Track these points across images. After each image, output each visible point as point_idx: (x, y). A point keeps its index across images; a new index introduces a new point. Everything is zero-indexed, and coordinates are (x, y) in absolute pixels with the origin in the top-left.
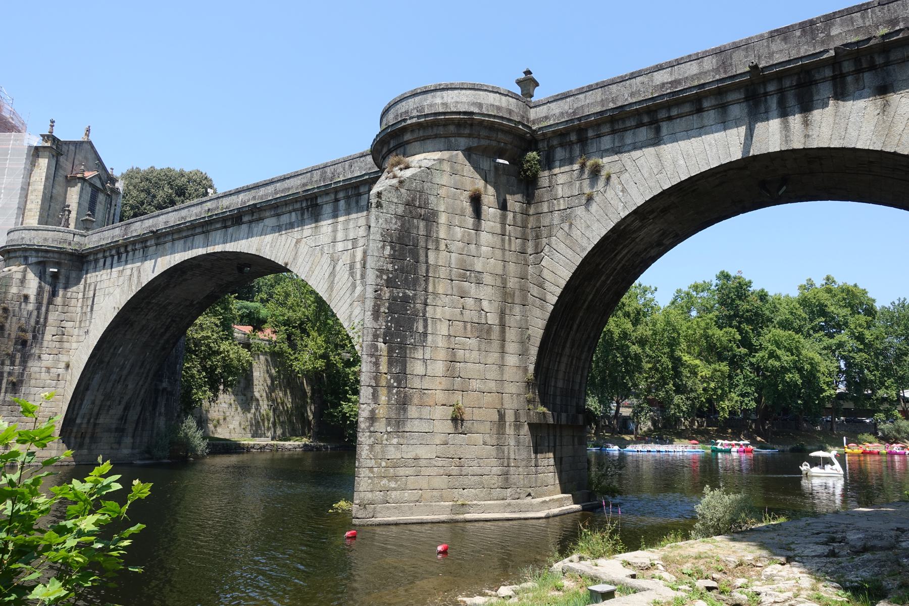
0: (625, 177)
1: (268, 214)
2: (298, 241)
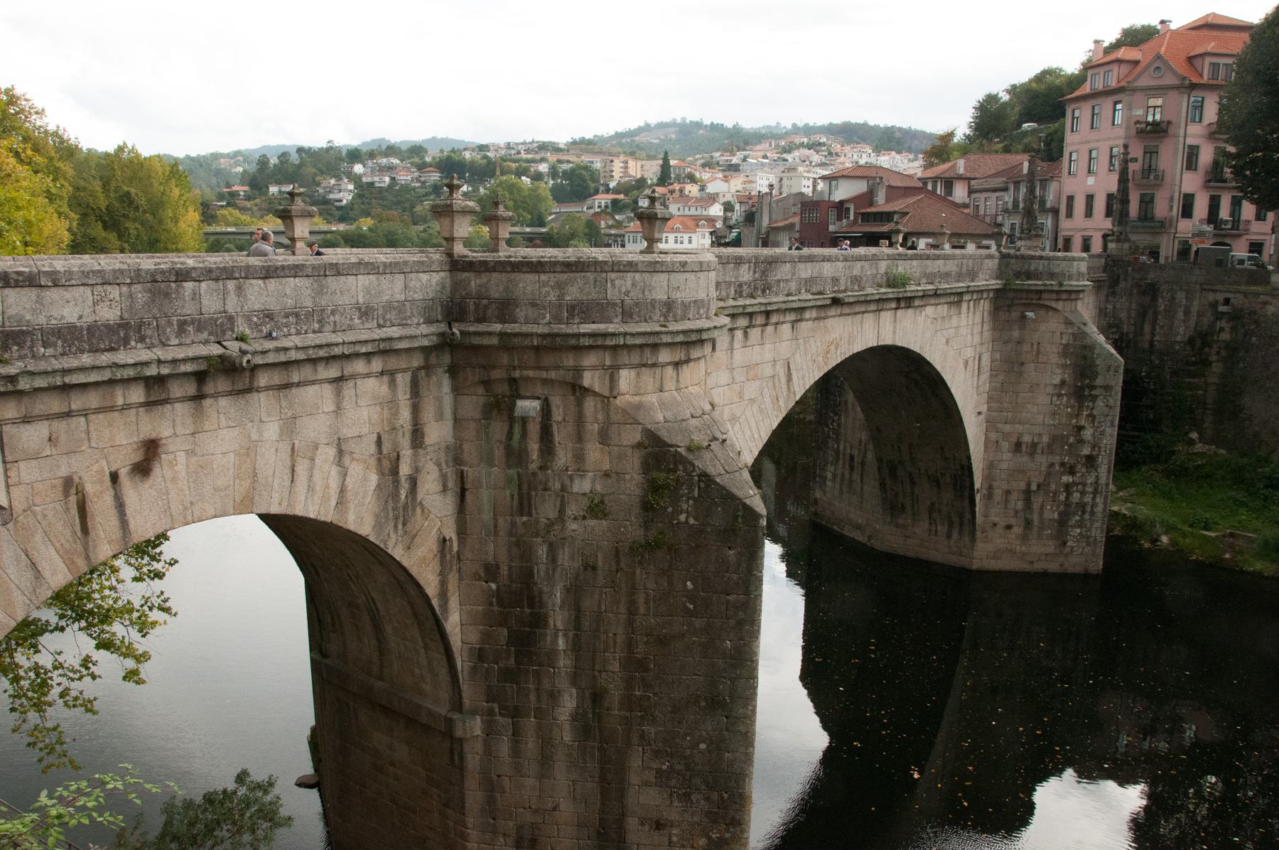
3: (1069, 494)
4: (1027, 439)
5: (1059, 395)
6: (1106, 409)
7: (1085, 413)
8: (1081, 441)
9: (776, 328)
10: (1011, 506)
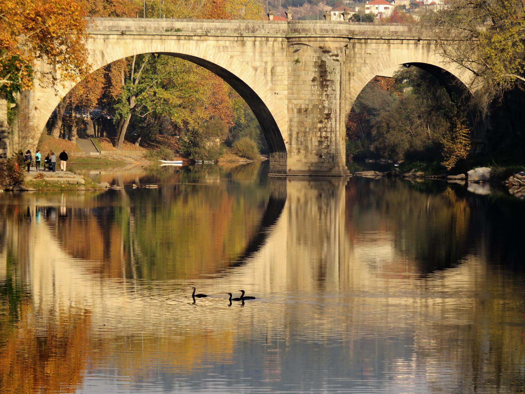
0: (379, 60)
4: (303, 107)
6: (332, 91)
7: (325, 93)
10: (299, 139)
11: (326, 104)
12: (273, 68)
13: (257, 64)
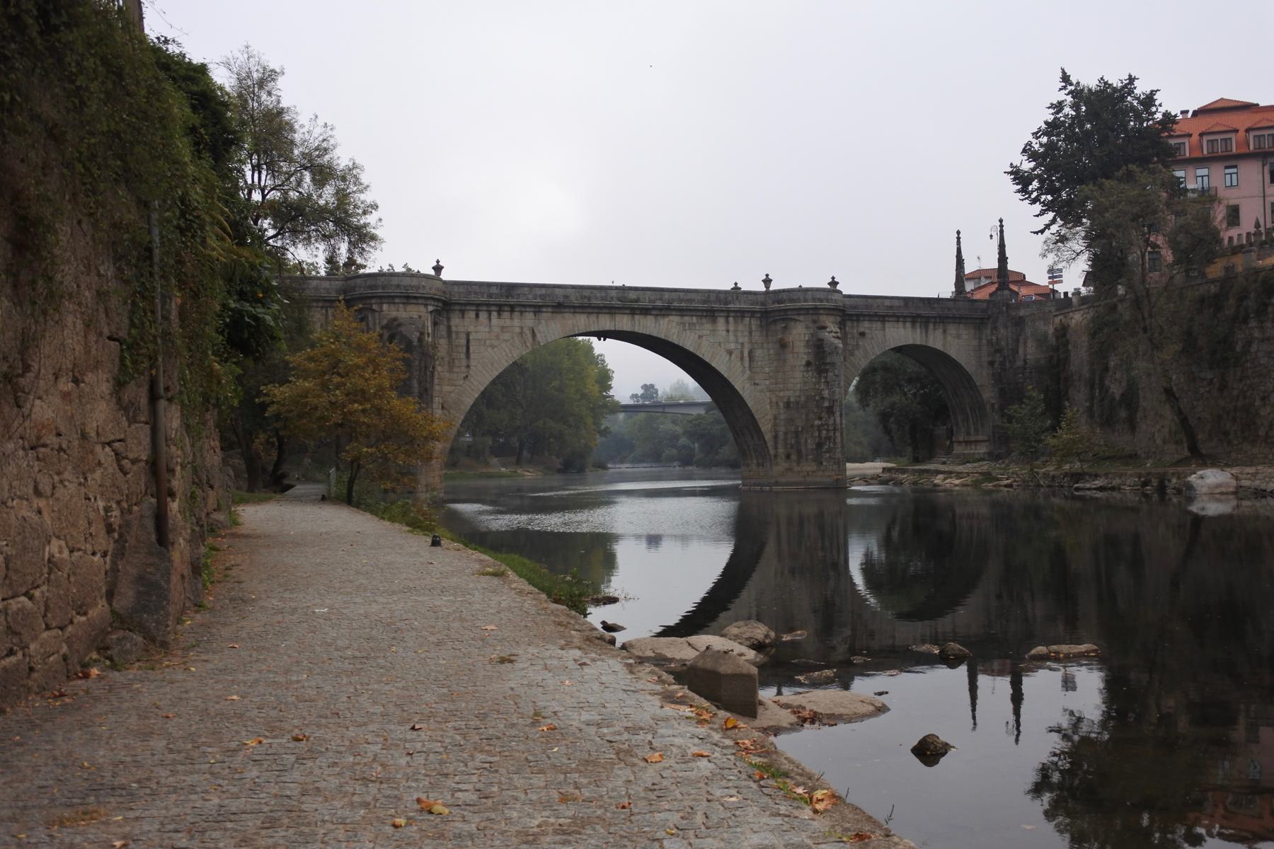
0: (873, 341)
1: (674, 313)
2: (700, 337)
3: (820, 432)
5: (807, 371)
8: (823, 398)
9: (521, 314)
11: (826, 393)
12: (750, 353)
13: (732, 346)
